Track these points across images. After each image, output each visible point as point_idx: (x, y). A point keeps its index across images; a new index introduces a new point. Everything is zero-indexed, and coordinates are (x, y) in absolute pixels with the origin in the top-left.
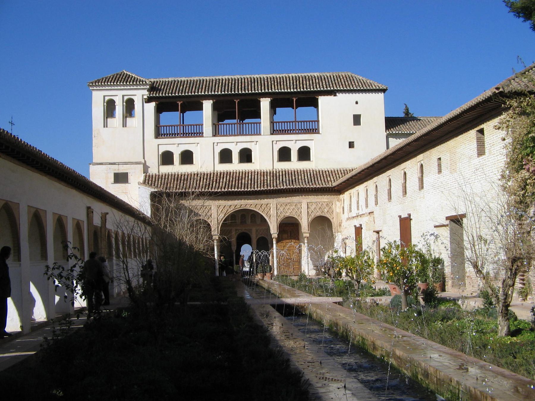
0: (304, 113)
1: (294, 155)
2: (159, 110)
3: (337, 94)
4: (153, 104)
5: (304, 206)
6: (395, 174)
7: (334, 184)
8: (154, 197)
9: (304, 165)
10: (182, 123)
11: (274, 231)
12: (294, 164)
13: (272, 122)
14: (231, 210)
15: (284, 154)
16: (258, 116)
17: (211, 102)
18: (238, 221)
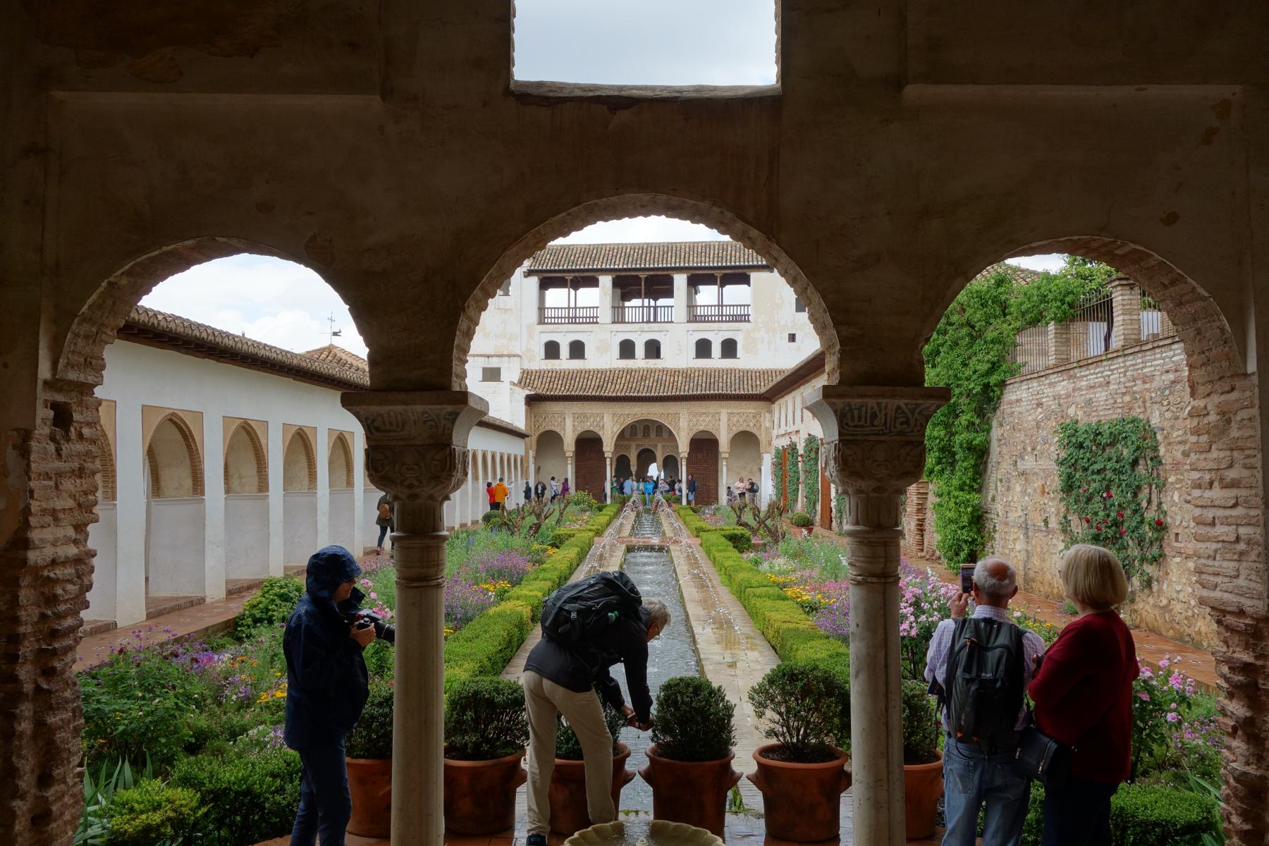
1: (716, 350)
5: (724, 417)
7: (763, 390)
8: (531, 401)
10: (572, 305)
12: (716, 361)
13: (691, 306)
14: (629, 421)
15: (703, 348)
18: (640, 435)
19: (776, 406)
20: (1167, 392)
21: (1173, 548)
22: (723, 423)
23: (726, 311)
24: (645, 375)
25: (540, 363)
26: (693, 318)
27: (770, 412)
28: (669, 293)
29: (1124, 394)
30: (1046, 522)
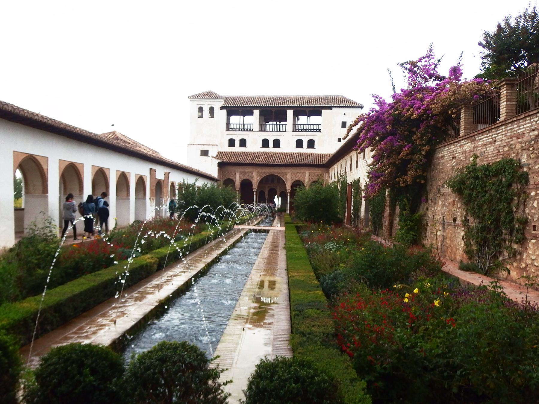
0: (314, 119)
1: (305, 144)
2: (229, 114)
3: (333, 109)
4: (224, 112)
5: (307, 175)
6: (348, 158)
8: (220, 165)
9: (310, 151)
11: (289, 187)
12: (305, 150)
13: (294, 125)
14: (265, 175)
15: (299, 144)
16: (286, 121)
17: (258, 111)
19: (330, 170)
20: (533, 142)
21: (531, 234)
22: (307, 176)
23: (311, 127)
24: (271, 155)
25: (225, 148)
26: (295, 130)
27: (328, 172)
28: (284, 118)
29: (504, 146)
30: (455, 220)
